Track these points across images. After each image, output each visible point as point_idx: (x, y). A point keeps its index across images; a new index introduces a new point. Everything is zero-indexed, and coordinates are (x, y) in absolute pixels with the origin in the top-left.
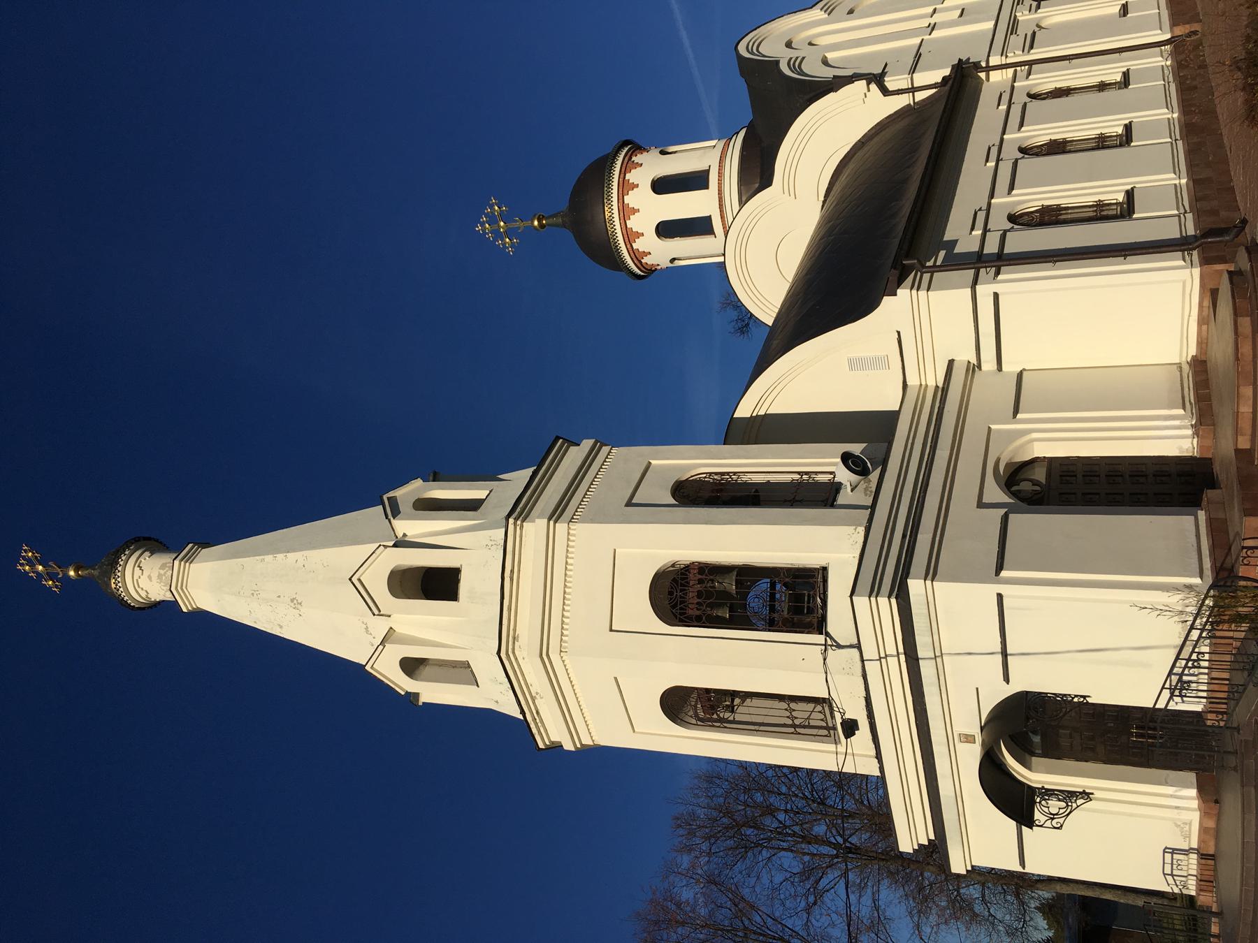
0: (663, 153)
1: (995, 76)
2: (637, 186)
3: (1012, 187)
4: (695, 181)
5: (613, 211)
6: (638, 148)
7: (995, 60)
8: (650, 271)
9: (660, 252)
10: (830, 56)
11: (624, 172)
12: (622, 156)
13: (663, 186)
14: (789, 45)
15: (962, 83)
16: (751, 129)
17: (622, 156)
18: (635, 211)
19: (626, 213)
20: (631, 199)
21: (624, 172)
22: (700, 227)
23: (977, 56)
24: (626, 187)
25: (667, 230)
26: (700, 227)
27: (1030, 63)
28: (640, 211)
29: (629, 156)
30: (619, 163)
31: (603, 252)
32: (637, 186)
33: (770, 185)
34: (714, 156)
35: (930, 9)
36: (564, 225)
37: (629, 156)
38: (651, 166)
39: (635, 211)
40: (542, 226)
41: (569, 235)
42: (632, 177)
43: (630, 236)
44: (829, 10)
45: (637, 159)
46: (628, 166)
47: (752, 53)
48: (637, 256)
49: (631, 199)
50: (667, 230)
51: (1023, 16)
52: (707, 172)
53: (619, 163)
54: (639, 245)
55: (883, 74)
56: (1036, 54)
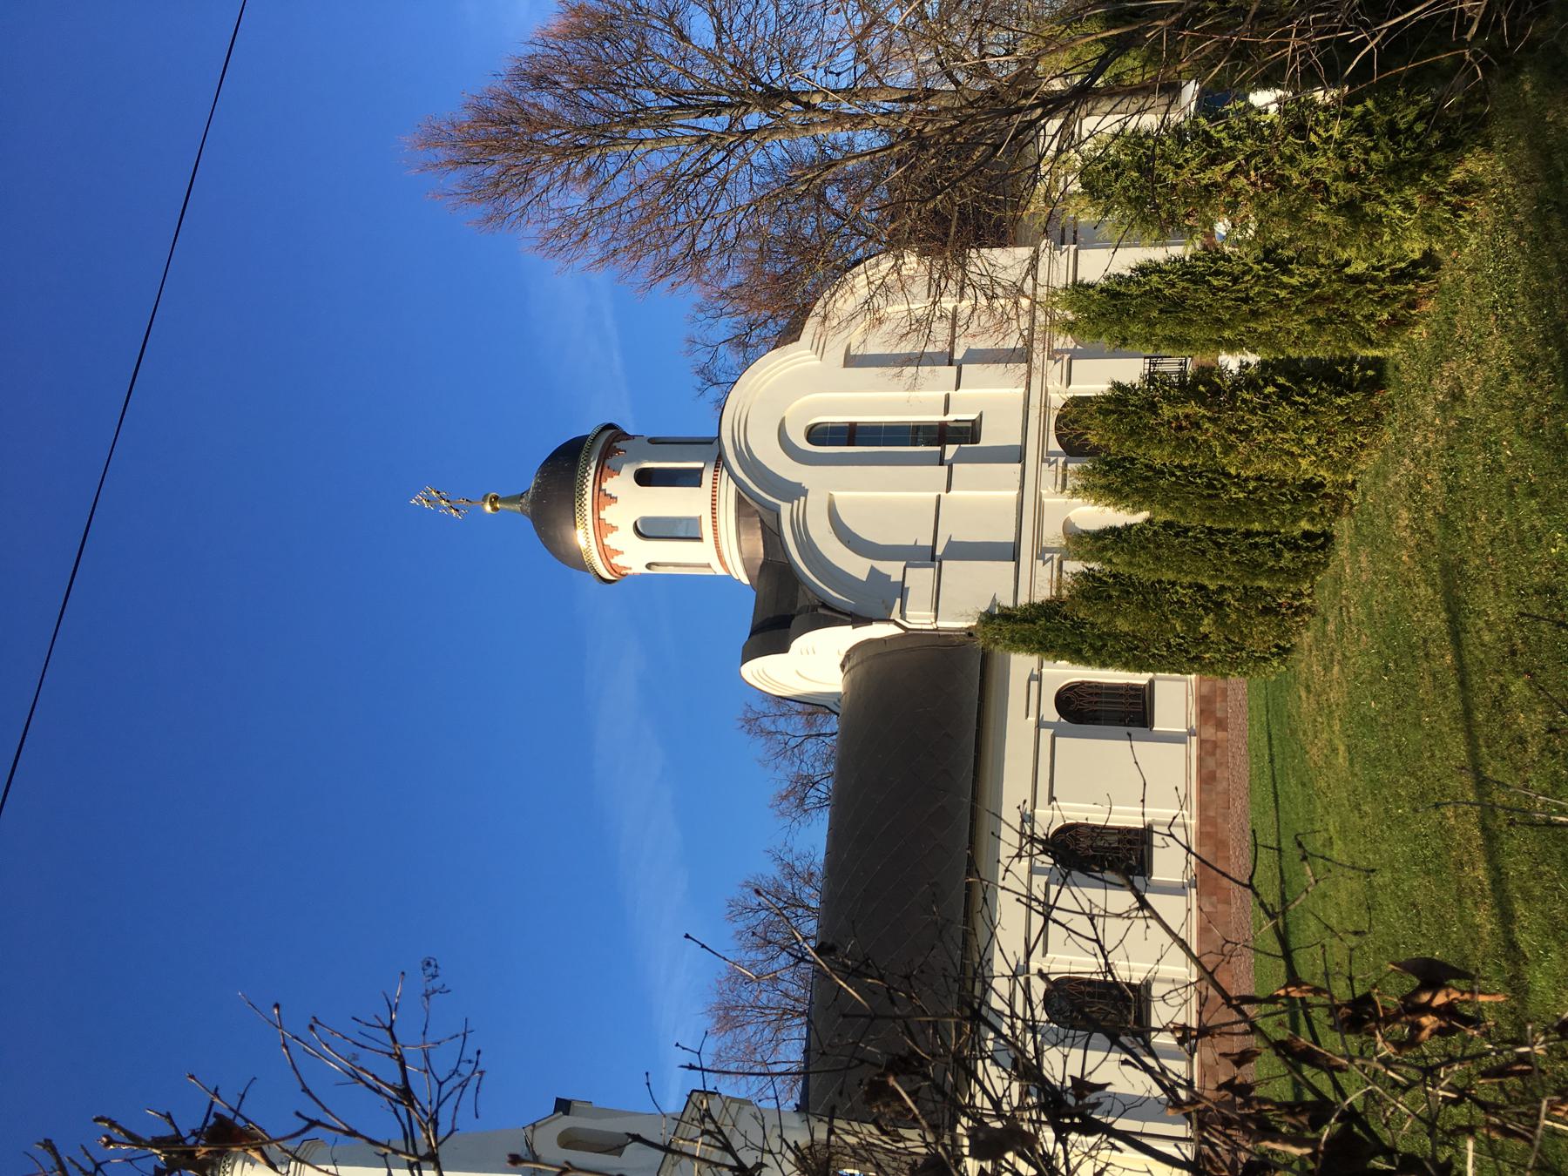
2: (614, 528)
3: (1044, 955)
10: (837, 494)
11: (597, 508)
12: (589, 490)
13: (647, 530)
17: (589, 490)
18: (618, 553)
20: (611, 541)
21: (597, 508)
29: (599, 481)
30: (588, 496)
32: (614, 528)
33: (783, 648)
35: (943, 394)
37: (599, 481)
42: (608, 514)
44: (820, 351)
46: (604, 498)
47: (739, 455)
49: (611, 541)
52: (696, 521)
53: (588, 496)
55: (902, 591)
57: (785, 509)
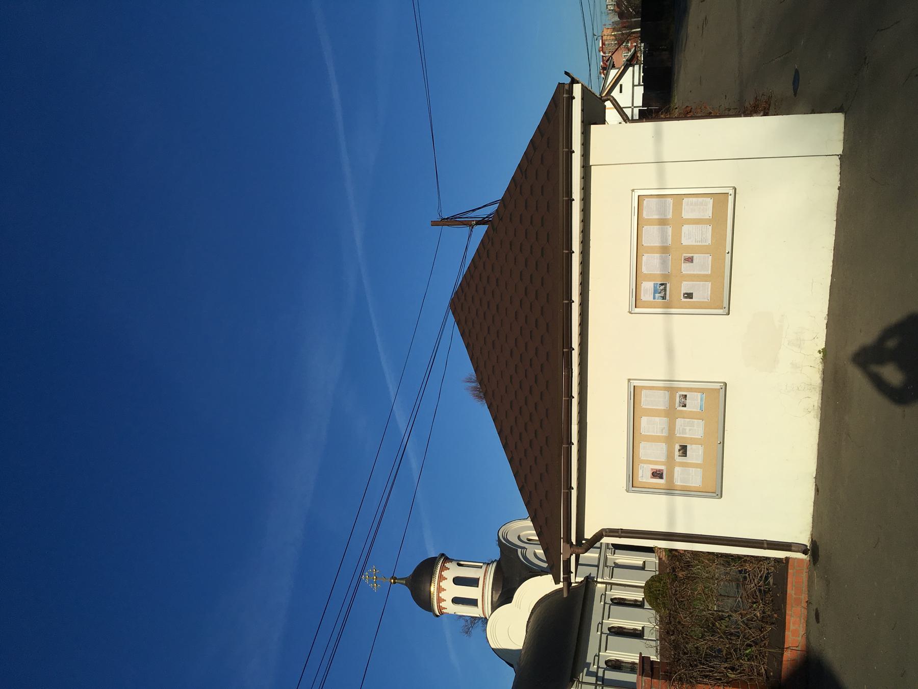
0: (459, 565)
1: (599, 585)
4: (473, 582)
5: (433, 589)
6: (447, 559)
7: (599, 580)
8: (442, 614)
9: (451, 609)
13: (458, 581)
14: (519, 537)
15: (589, 582)
16: (499, 563)
18: (444, 590)
19: (440, 589)
22: (473, 602)
23: (593, 571)
24: (441, 578)
25: (456, 601)
26: (473, 602)
27: (612, 584)
28: (445, 590)
29: (444, 563)
31: (425, 602)
34: (487, 576)
36: (406, 585)
37: (444, 563)
38: (453, 571)
39: (444, 590)
40: (395, 583)
41: (407, 591)
42: (445, 574)
43: (440, 600)
45: (447, 565)
46: (444, 568)
48: (440, 608)
50: (456, 601)
51: (609, 556)
54: (442, 604)
56: (614, 581)
57: (519, 550)
